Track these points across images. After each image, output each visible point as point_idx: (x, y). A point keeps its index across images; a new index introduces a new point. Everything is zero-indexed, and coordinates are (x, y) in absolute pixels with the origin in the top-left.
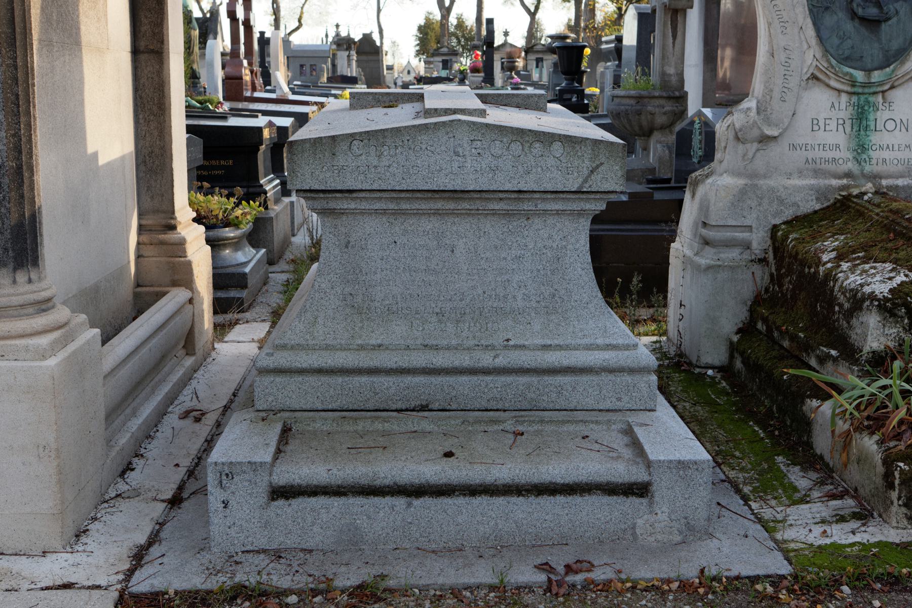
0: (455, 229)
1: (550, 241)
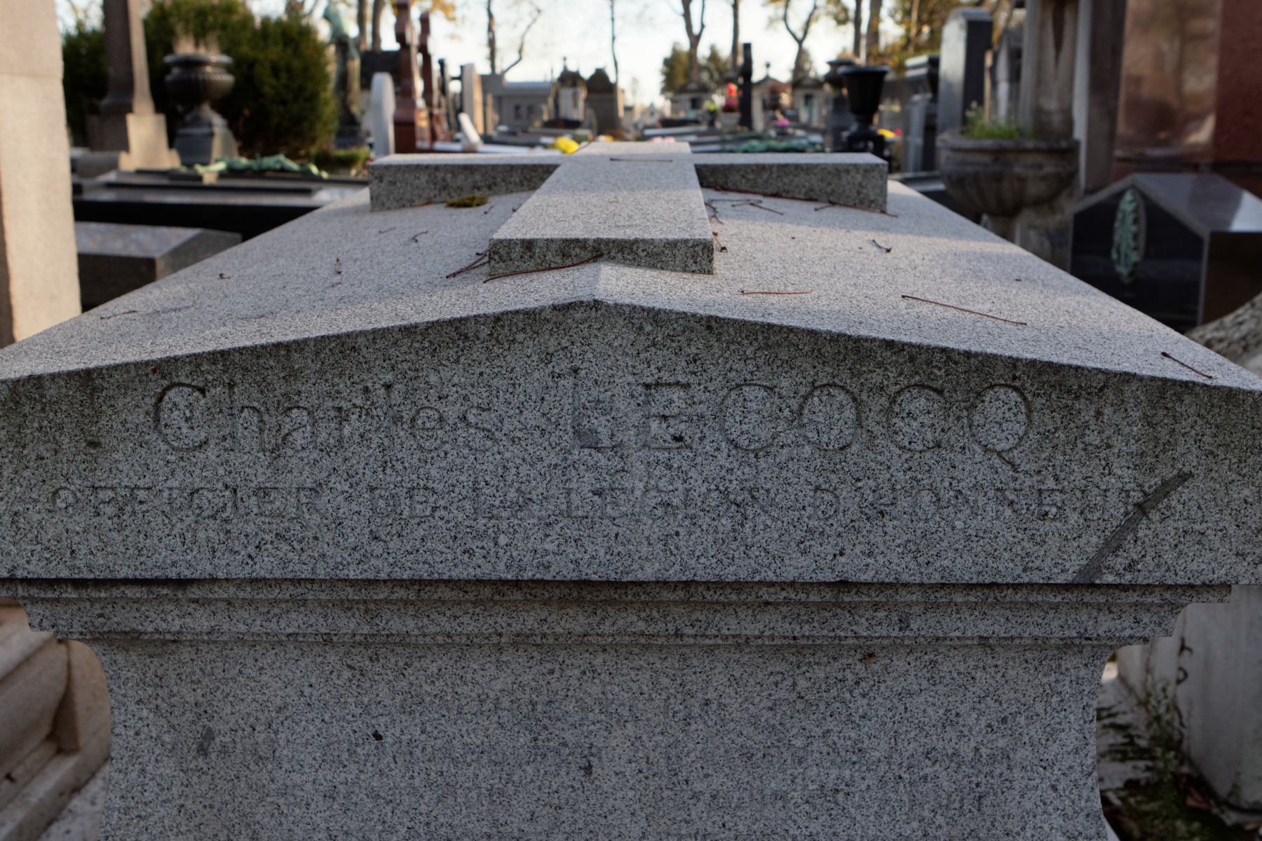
0: (595, 689)
1: (951, 733)
